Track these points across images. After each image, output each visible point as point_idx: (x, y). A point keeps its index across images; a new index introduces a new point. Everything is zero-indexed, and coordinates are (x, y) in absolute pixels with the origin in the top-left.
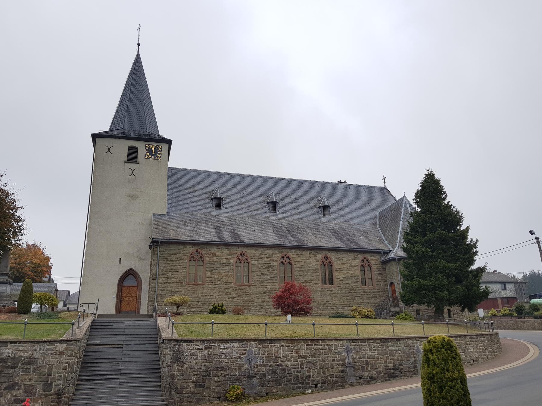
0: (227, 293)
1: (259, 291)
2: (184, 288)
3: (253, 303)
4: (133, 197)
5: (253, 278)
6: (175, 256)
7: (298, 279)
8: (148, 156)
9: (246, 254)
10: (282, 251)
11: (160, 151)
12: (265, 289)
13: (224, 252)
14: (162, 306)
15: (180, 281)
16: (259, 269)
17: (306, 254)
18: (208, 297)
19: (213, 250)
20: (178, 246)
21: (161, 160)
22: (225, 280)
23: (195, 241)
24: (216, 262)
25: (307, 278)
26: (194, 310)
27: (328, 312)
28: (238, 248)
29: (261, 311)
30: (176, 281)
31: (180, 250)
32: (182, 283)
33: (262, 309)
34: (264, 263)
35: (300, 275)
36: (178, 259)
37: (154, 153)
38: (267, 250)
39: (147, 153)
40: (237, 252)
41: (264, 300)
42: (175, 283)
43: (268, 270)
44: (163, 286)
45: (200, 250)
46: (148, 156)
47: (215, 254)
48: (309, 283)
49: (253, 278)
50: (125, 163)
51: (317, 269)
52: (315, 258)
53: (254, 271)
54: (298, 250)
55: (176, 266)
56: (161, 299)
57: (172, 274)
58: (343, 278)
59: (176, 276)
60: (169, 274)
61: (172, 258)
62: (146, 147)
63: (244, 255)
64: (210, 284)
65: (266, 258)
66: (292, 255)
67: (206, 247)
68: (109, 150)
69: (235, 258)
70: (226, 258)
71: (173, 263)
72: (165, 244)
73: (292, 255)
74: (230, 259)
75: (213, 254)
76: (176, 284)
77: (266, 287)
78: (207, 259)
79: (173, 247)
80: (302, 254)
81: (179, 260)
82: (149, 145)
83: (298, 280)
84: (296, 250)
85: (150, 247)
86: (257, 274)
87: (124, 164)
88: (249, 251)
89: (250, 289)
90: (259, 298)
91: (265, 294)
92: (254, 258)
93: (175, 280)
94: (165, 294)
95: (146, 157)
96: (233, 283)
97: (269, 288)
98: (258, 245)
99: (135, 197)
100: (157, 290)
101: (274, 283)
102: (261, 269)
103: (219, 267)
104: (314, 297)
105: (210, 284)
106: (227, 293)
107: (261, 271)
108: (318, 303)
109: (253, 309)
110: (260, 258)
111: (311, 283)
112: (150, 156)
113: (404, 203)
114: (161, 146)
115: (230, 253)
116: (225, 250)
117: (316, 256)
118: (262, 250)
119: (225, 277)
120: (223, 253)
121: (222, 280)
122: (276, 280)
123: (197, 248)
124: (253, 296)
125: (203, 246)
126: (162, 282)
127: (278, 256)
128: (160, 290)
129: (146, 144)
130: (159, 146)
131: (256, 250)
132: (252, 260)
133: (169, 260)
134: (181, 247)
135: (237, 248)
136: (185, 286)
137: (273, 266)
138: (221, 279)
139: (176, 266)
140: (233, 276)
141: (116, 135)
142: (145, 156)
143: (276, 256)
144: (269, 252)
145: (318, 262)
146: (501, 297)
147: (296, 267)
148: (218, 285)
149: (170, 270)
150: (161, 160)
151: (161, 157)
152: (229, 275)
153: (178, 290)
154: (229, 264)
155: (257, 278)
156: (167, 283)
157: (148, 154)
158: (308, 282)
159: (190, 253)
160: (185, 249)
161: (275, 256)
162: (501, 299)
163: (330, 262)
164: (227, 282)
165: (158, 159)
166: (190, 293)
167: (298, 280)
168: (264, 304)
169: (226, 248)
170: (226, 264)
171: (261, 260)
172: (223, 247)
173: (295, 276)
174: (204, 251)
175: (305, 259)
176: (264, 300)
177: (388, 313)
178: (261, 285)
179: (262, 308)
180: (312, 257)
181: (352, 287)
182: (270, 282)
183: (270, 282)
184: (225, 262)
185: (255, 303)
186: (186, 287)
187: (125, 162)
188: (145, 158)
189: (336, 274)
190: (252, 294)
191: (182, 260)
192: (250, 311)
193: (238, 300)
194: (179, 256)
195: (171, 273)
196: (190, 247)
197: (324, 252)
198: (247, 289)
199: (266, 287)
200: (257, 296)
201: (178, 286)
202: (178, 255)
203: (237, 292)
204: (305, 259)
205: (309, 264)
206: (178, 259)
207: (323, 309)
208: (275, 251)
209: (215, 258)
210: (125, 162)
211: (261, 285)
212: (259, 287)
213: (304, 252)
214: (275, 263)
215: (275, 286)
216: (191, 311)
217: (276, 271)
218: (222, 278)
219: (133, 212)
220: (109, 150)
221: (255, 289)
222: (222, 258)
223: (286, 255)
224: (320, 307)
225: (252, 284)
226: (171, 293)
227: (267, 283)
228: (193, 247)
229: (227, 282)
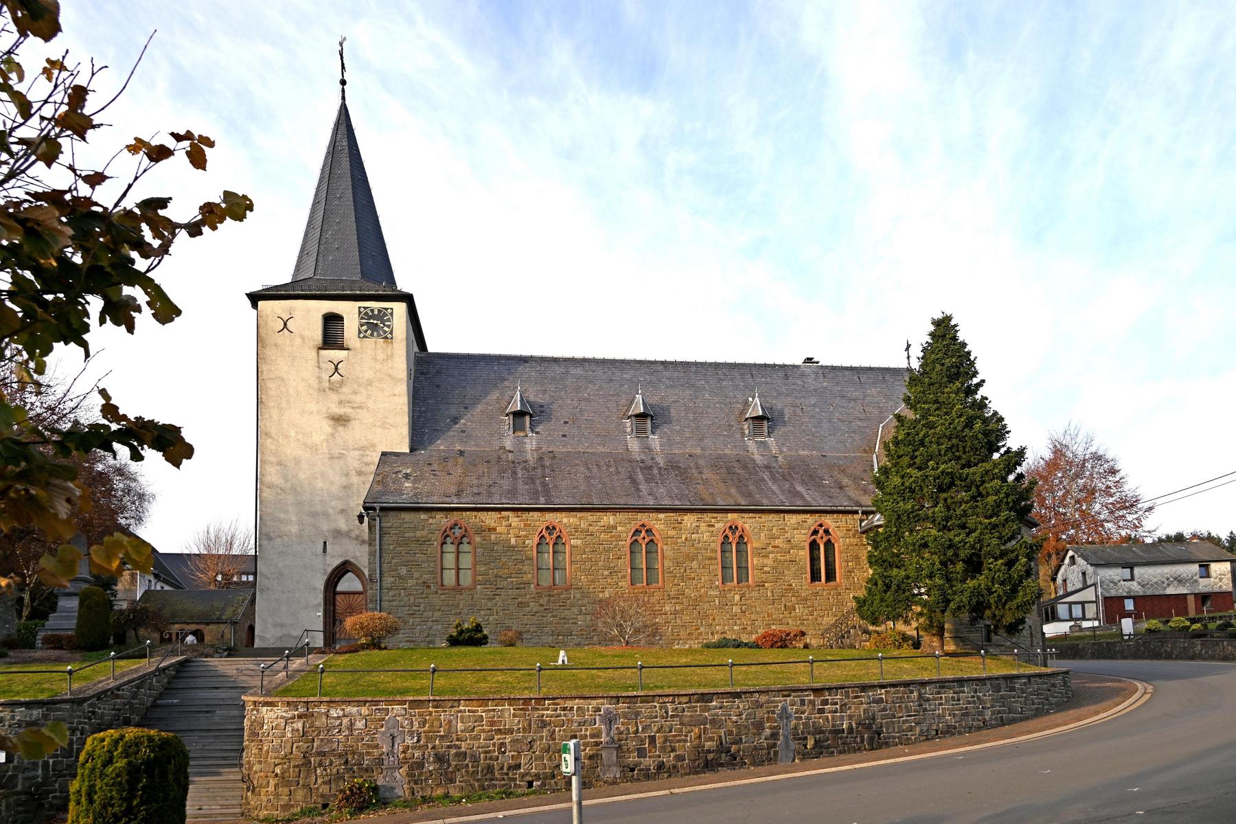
0: (521, 605)
6: (412, 535)
8: (366, 331)
11: (389, 320)
12: (601, 595)
18: (482, 612)
32: (429, 587)
39: (362, 325)
44: (391, 593)
46: (366, 331)
47: (495, 529)
55: (415, 554)
58: (769, 569)
60: (403, 571)
61: (406, 540)
64: (486, 588)
68: (285, 324)
69: (536, 536)
71: (408, 548)
78: (478, 539)
87: (318, 353)
95: (362, 335)
96: (532, 586)
99: (344, 420)
100: (381, 601)
105: (486, 588)
106: (521, 605)
112: (369, 332)
115: (525, 525)
121: (509, 579)
122: (624, 577)
126: (389, 585)
133: (401, 543)
136: (437, 593)
139: (415, 554)
142: (360, 332)
144: (609, 519)
146: (1197, 591)
147: (665, 549)
148: (501, 589)
150: (392, 338)
151: (391, 333)
157: (365, 328)
159: (443, 529)
162: (1195, 597)
163: (741, 537)
164: (521, 584)
181: (791, 585)
185: (580, 623)
189: (753, 561)
193: (543, 616)
197: (730, 516)
201: (422, 593)
202: (419, 534)
203: (541, 601)
208: (621, 517)
220: (285, 324)
221: (578, 596)
229: (521, 584)
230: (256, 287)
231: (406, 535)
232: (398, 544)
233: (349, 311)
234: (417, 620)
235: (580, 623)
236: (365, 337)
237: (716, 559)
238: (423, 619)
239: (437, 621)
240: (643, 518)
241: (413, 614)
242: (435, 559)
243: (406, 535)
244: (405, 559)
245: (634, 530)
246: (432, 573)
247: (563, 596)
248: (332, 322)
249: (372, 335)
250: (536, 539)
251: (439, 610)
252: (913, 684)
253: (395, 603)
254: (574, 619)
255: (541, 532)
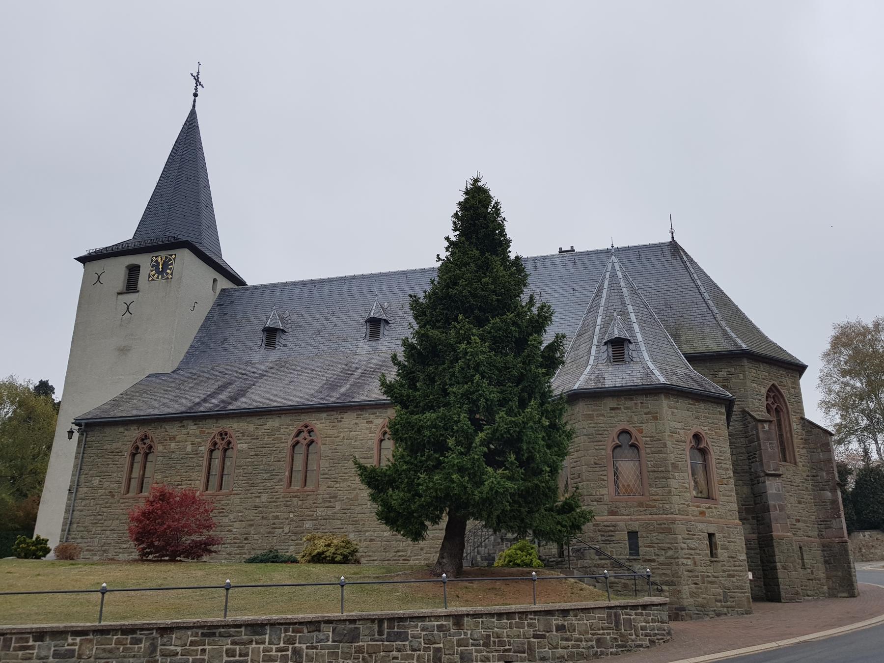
1: (245, 504)
2: (115, 505)
3: (230, 531)
4: (124, 350)
5: (236, 479)
6: (109, 447)
7: (326, 474)
8: (153, 276)
9: (229, 431)
10: (299, 418)
11: (171, 264)
12: (257, 500)
13: (191, 431)
14: (77, 539)
15: (110, 492)
16: (250, 460)
17: (349, 419)
19: (172, 430)
20: (116, 429)
21: (149, 281)
22: (186, 486)
23: (140, 416)
24: (173, 452)
25: (346, 471)
26: (125, 546)
27: (383, 544)
28: (217, 421)
29: (242, 547)
30: (105, 493)
31: (118, 436)
32: (113, 496)
33: (246, 542)
34: (261, 448)
35: (332, 465)
36: (113, 452)
37: (161, 270)
38: (271, 420)
39: (152, 271)
40: (213, 429)
41: (252, 522)
42: (102, 497)
43: (268, 460)
45: (151, 434)
46: (153, 276)
47: (174, 438)
48: (348, 483)
49: (236, 479)
50: (120, 296)
51: (371, 449)
52: (368, 426)
53: (239, 464)
54: (332, 413)
55: (108, 465)
56: (77, 526)
57: (100, 481)
59: (106, 484)
60: (96, 481)
62: (152, 261)
63: (226, 434)
65: (267, 436)
66: (319, 425)
67: (161, 426)
70: (192, 444)
72: (98, 428)
73: (319, 425)
74: (200, 445)
75: (170, 438)
76: (104, 499)
77: (260, 497)
79: (109, 432)
80: (341, 421)
81: (114, 454)
82: (156, 257)
83: (326, 476)
84: (329, 413)
85: (71, 433)
86: (245, 470)
88: (235, 426)
89: (228, 502)
90: (243, 519)
91: (256, 511)
92: (244, 438)
93: (104, 491)
94: (84, 517)
95: (151, 279)
97: (264, 498)
98: (248, 412)
100: (73, 511)
101: (276, 487)
102: (253, 460)
103: (179, 462)
104: (356, 511)
107: (255, 463)
108: (364, 524)
109: (228, 541)
110: (255, 437)
111: (354, 482)
113: (609, 268)
114: (175, 255)
115: (200, 432)
116: (192, 428)
117: (371, 421)
118: (260, 422)
119: (186, 480)
120: (188, 434)
121: (179, 487)
122: (280, 481)
123: (146, 430)
124: (231, 516)
125: (156, 424)
127: (290, 430)
128: (78, 510)
129: (153, 257)
130: (171, 255)
131: (248, 423)
132: (239, 444)
134: (121, 429)
135: (215, 421)
137: (278, 452)
138: (178, 485)
139: (108, 465)
140: (199, 478)
141: (109, 252)
142: (150, 276)
143: (287, 430)
144: (273, 423)
145: (373, 435)
147: (323, 447)
149: (98, 474)
152: (195, 475)
153: (105, 510)
154: (197, 454)
155: (245, 478)
156: (91, 498)
158: (347, 480)
160: (126, 432)
161: (284, 430)
165: (168, 278)
166: (124, 514)
167: (326, 476)
168: (252, 530)
169: (195, 425)
170: (191, 456)
171: (257, 441)
172: (191, 423)
173: (321, 469)
174: (155, 433)
175: (346, 430)
176: (252, 522)
177: (499, 543)
178: (251, 491)
179: (246, 539)
180: (363, 425)
182: (269, 485)
183: (269, 485)
184: (190, 450)
185: (235, 530)
186: (119, 504)
187: (119, 294)
188: (149, 281)
190: (231, 512)
191: (119, 454)
192: (223, 546)
194: (115, 447)
195: (99, 478)
196: (135, 429)
198: (223, 502)
199: (260, 497)
200: (240, 514)
201: (107, 503)
202: (115, 445)
204: (346, 430)
205: (353, 441)
206: (113, 452)
207: (373, 538)
208: (286, 419)
209: (173, 445)
210: (119, 294)
211: (251, 491)
212: (246, 496)
213: (345, 416)
214: (283, 445)
215: (277, 492)
216: (120, 549)
217: (283, 461)
218: (180, 483)
219: (122, 375)
222: (186, 443)
223: (306, 427)
224: (367, 534)
225: (233, 492)
226: (95, 515)
227: (262, 487)
228: (140, 428)
230: (83, 253)
231: (105, 447)
232: (97, 456)
233: (144, 262)
234: (99, 528)
235: (235, 530)
236: (153, 280)
237: (371, 458)
238: (104, 528)
239: (113, 530)
240: (306, 419)
241: (96, 523)
242: (122, 469)
243: (105, 447)
244: (100, 470)
245: (295, 431)
246: (119, 482)
247: (223, 502)
248: (133, 271)
249: (158, 277)
250: (208, 445)
251: (117, 519)
252: (142, 629)
253: (84, 513)
254: (231, 526)
255: (214, 438)
